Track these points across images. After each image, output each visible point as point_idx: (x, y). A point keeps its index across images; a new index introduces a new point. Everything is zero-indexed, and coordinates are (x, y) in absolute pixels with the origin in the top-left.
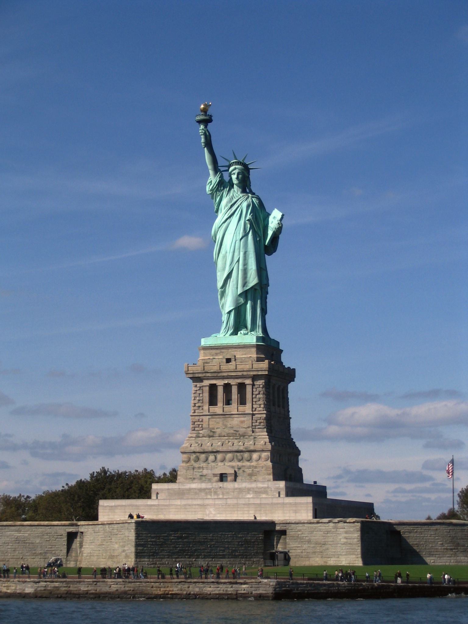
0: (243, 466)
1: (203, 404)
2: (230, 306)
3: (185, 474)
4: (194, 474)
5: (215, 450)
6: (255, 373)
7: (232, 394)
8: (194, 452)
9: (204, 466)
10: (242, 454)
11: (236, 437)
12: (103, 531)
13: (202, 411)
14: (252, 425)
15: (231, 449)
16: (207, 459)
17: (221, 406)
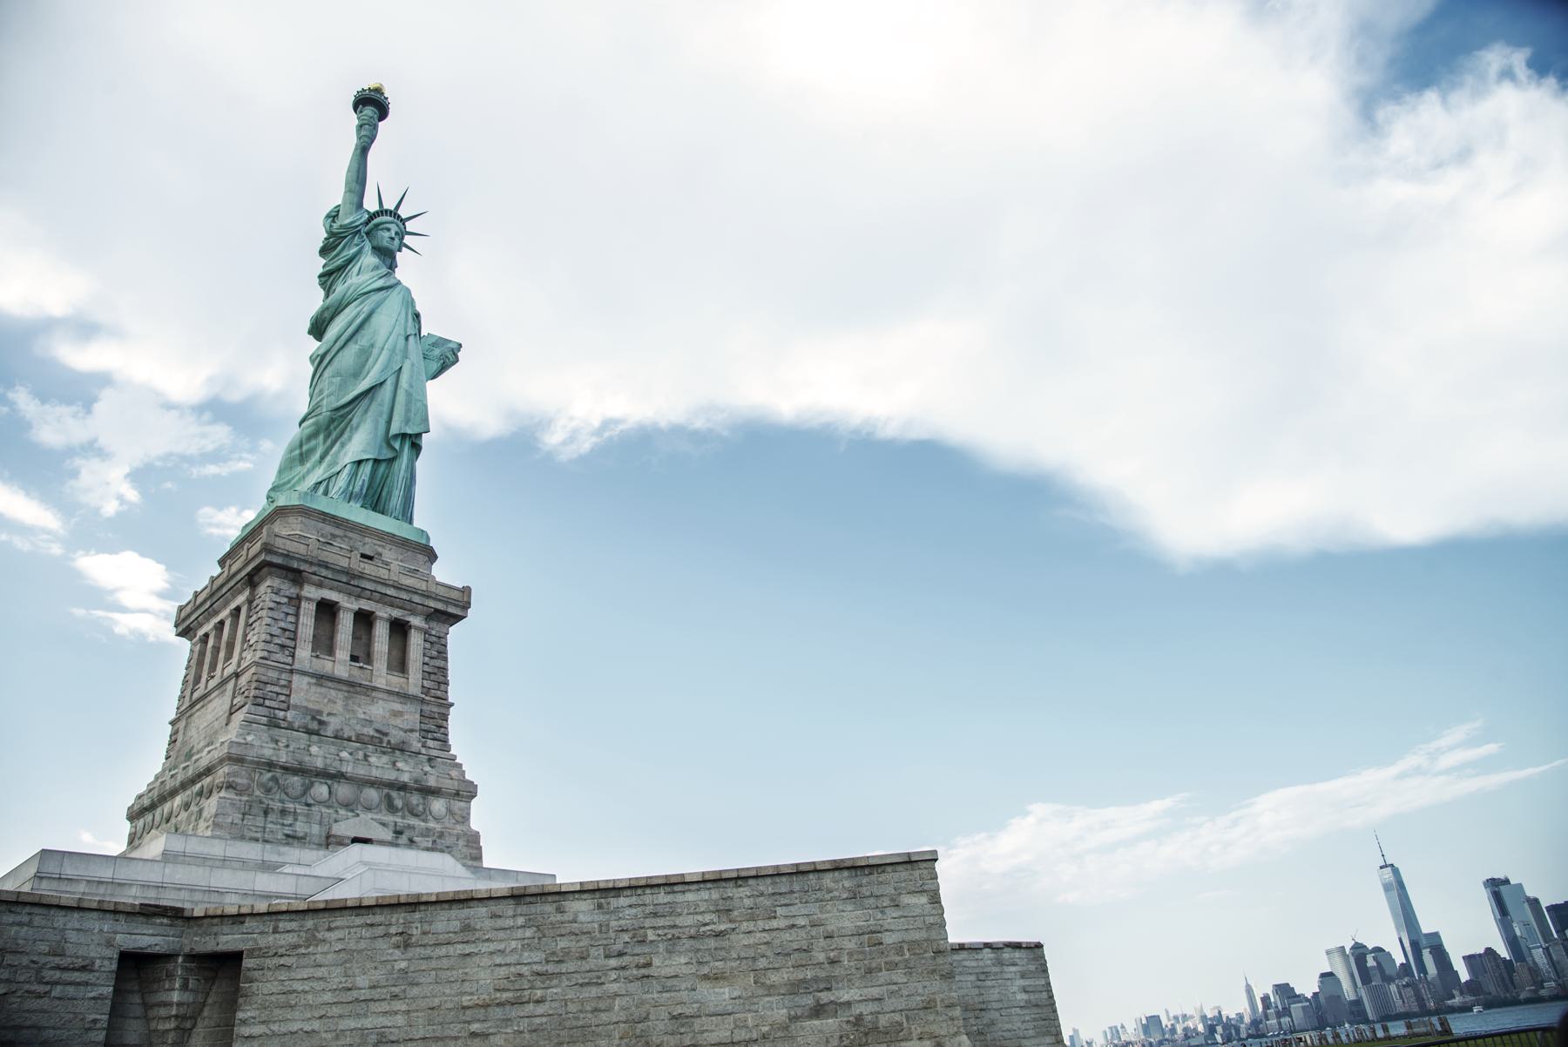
0: (410, 827)
1: (294, 643)
2: (364, 451)
3: (236, 824)
4: (267, 830)
5: (332, 771)
6: (440, 606)
7: (377, 639)
8: (271, 765)
9: (298, 811)
10: (402, 793)
11: (383, 749)
12: (529, 933)
13: (289, 660)
14: (421, 730)
15: (375, 773)
16: (304, 793)
17: (345, 661)
